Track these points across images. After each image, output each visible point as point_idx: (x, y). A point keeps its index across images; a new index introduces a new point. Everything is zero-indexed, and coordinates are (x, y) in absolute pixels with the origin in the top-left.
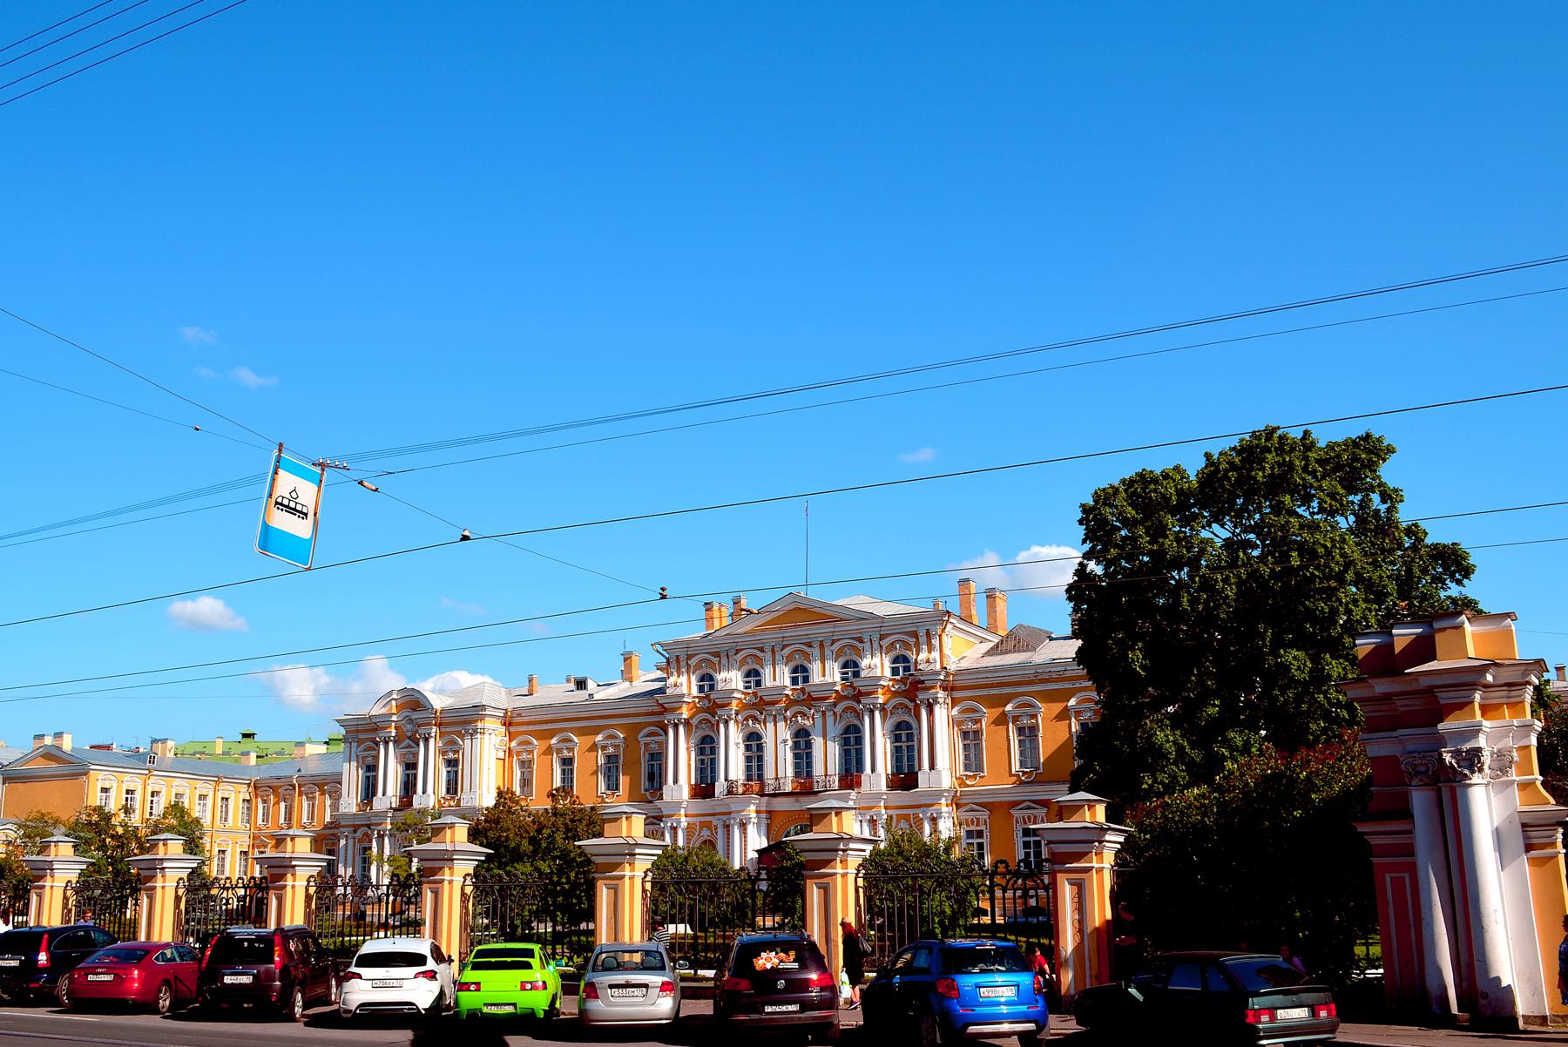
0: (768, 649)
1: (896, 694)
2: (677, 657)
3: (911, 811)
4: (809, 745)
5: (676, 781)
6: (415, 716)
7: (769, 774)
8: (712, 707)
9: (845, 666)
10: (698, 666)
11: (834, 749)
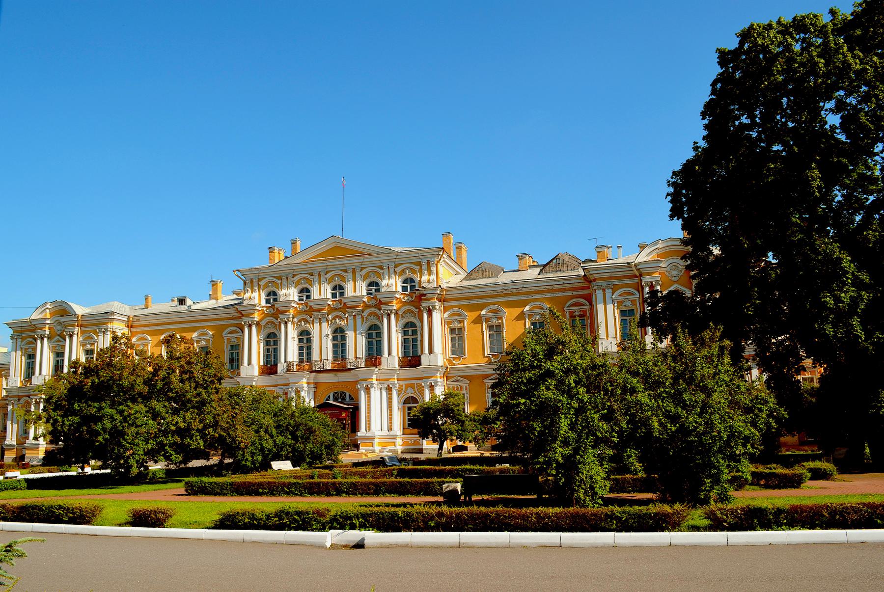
0: (316, 274)
1: (405, 303)
2: (251, 280)
3: (415, 382)
4: (343, 338)
5: (249, 363)
6: (62, 319)
7: (315, 357)
8: (276, 311)
9: (370, 285)
10: (266, 286)
11: (362, 341)
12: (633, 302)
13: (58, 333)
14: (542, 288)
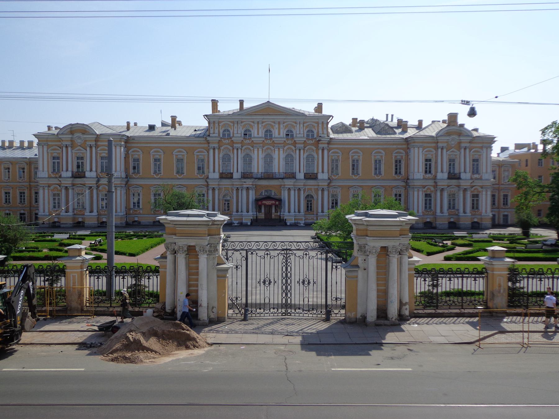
6: (85, 136)
12: (432, 155)
13: (79, 144)
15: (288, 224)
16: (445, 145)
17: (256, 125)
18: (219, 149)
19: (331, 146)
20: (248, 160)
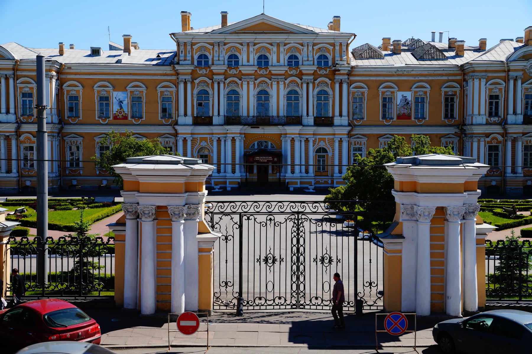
3: (326, 137)
12: (500, 90)
14: (426, 73)
15: (292, 189)
16: (520, 73)
17: (245, 48)
18: (192, 82)
19: (352, 78)
20: (233, 97)
